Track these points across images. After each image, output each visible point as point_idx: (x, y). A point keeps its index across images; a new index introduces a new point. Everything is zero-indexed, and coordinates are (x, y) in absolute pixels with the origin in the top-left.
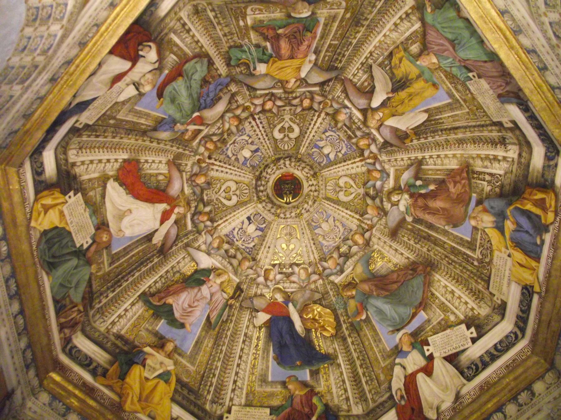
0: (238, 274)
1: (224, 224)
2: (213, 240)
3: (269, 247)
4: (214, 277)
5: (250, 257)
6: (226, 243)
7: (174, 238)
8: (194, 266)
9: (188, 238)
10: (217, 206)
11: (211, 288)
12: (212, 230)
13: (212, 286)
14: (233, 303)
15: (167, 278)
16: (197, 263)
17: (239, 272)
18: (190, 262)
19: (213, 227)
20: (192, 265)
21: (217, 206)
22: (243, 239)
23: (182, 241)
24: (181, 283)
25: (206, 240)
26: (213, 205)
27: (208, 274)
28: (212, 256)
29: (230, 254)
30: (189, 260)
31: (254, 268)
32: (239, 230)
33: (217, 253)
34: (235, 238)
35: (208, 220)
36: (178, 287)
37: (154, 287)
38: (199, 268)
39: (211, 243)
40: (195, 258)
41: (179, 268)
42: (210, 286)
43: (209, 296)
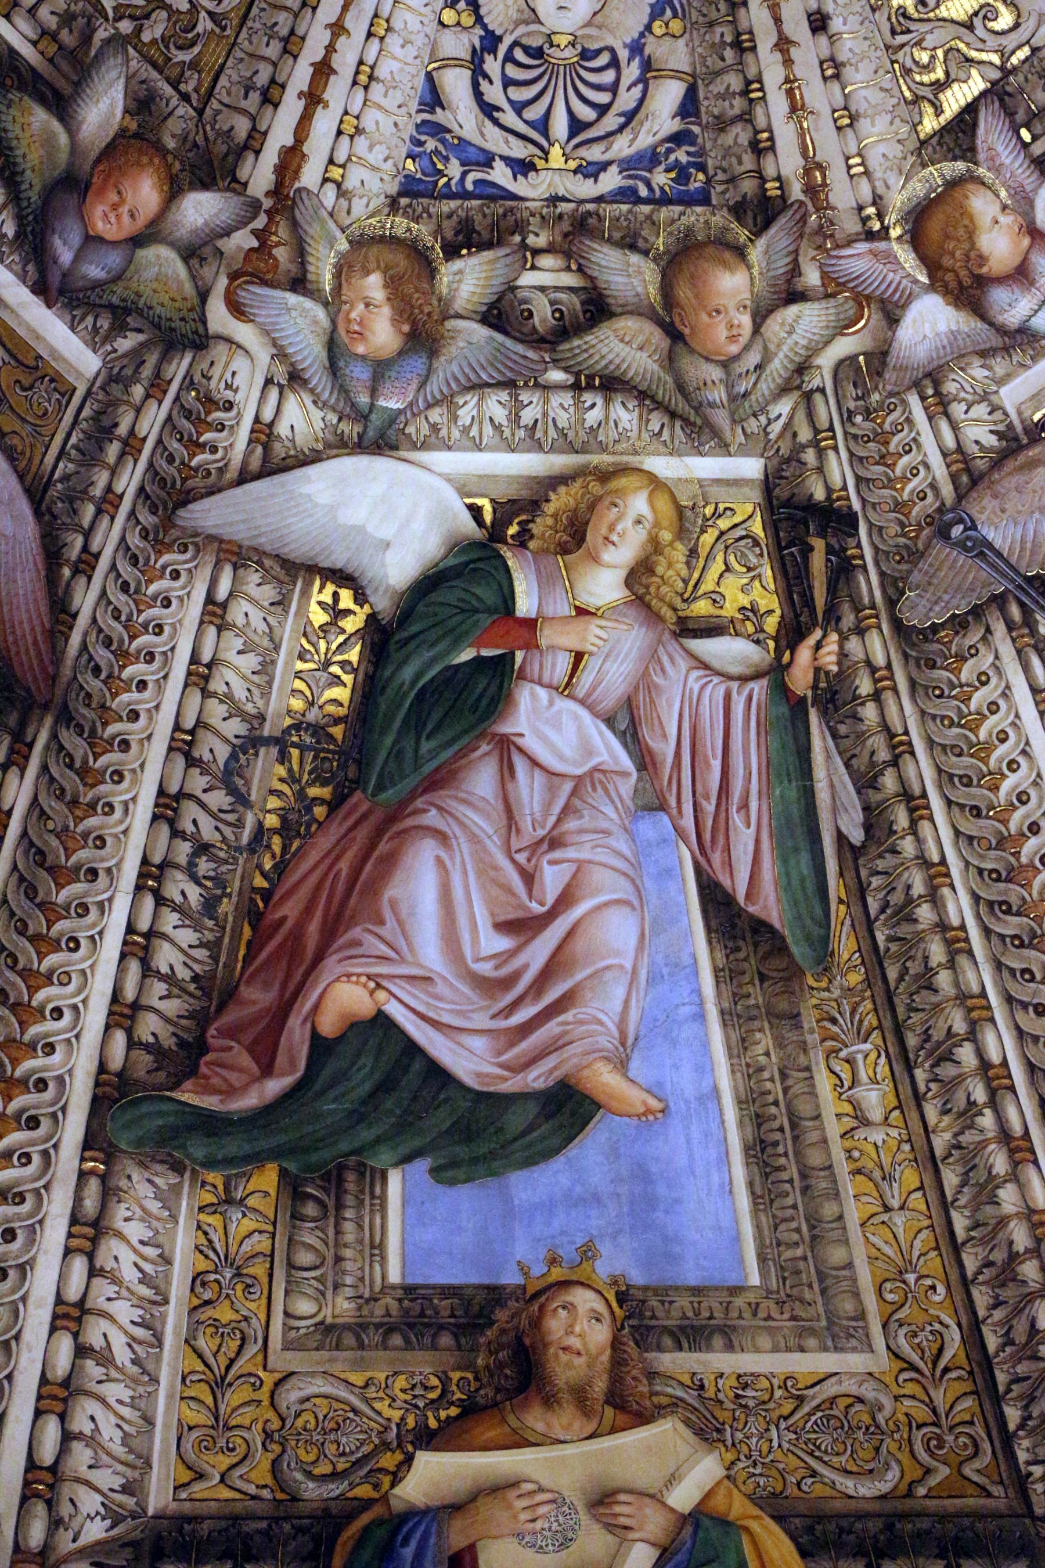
0: (721, 418)
1: (324, 124)
2: (334, 303)
3: (819, 22)
4: (545, 582)
5: (720, 219)
6: (452, 252)
7: (29, 529)
8: (338, 613)
9: (131, 445)
10: (155, 29)
11: (585, 680)
12: (260, 235)
13: (579, 657)
14: (829, 659)
15: (203, 848)
16: (342, 577)
17: (718, 394)
18: (281, 603)
19: (255, 206)
20: (319, 617)
21: (155, 29)
22: (560, 126)
23: (110, 501)
24: (333, 805)
25: (280, 354)
26: (115, 41)
27: (487, 594)
28: (417, 429)
29: (543, 314)
30: (268, 593)
31: (812, 277)
32: (478, 73)
33: (436, 386)
34: (487, 160)
35: (173, 192)
36: (334, 855)
37: (160, 988)
38: (382, 603)
39: (332, 345)
40: (298, 549)
41: (236, 711)
42: (562, 664)
43: (626, 763)
